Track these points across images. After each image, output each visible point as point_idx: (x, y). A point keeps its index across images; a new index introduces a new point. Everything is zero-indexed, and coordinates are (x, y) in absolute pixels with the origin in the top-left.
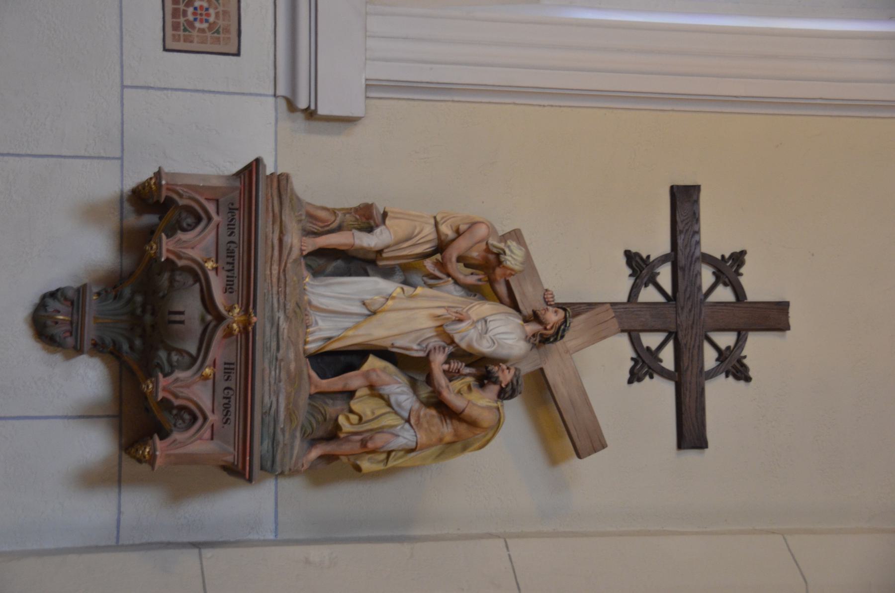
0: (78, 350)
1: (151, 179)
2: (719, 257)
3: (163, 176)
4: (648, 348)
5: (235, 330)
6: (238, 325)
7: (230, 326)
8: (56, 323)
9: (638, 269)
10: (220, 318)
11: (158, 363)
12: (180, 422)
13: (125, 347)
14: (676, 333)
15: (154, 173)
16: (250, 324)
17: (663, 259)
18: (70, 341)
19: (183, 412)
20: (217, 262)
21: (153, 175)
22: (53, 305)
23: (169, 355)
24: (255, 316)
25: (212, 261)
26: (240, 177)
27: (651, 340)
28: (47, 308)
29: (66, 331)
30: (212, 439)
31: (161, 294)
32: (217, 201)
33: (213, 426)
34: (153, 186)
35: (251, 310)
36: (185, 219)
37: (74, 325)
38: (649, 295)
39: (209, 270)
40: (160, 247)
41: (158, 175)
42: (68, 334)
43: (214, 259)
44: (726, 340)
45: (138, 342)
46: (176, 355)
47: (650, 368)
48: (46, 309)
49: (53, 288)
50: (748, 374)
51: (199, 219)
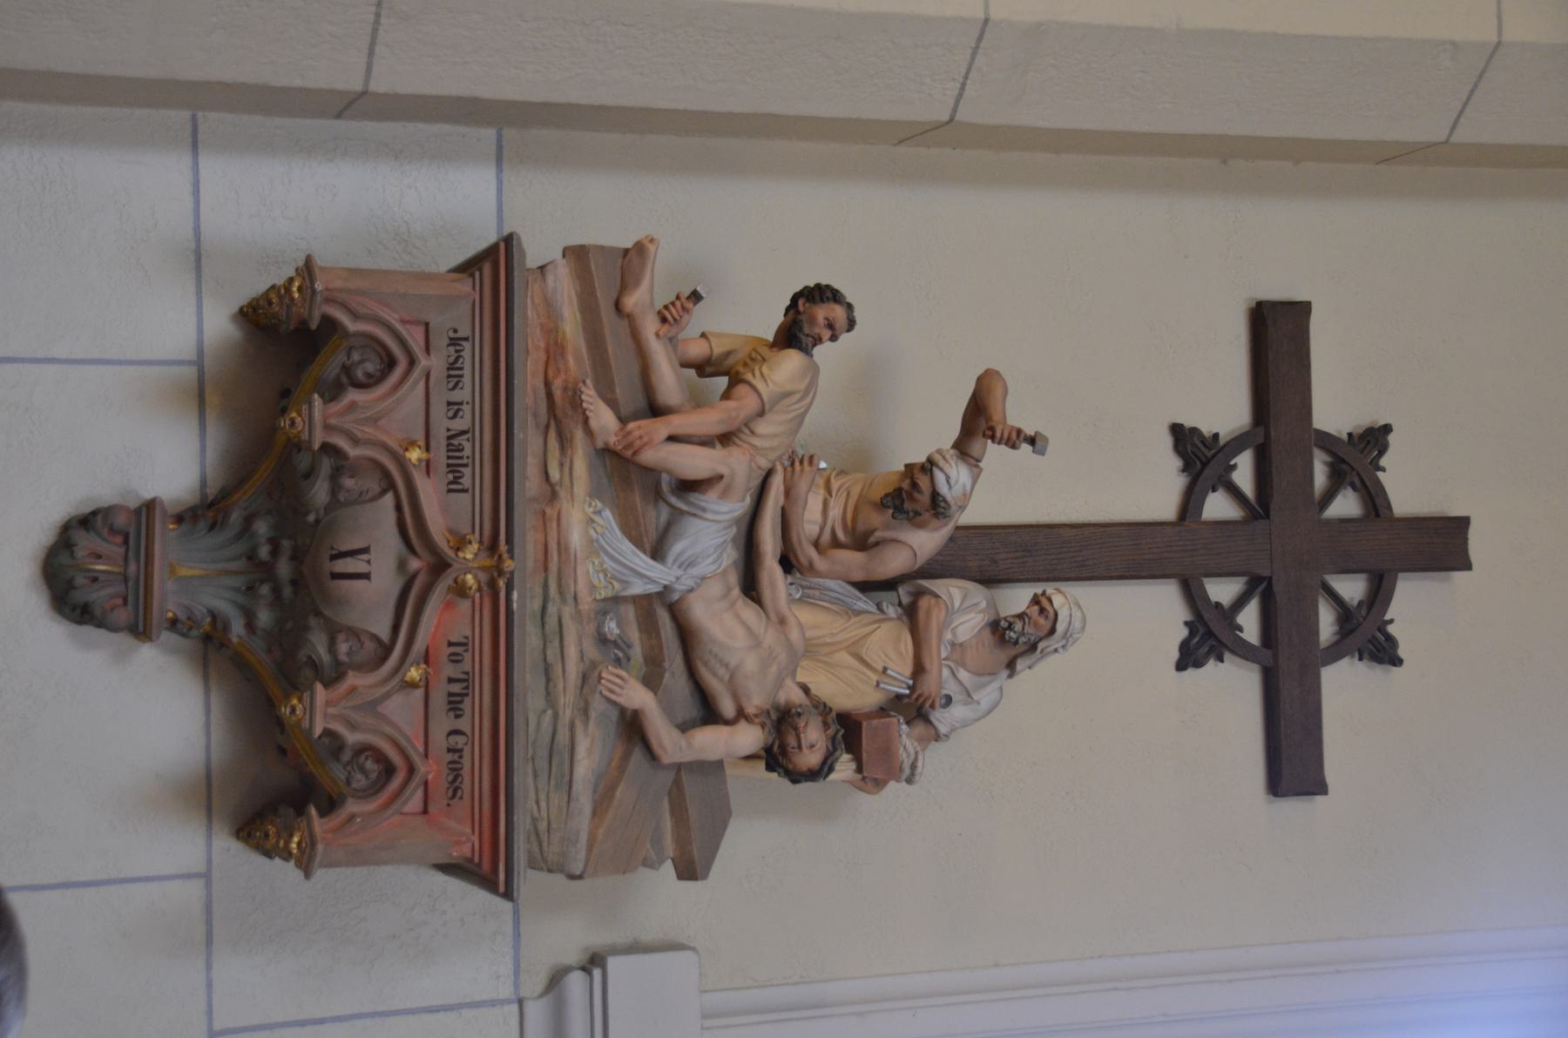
0: (141, 630)
1: (291, 280)
3: (317, 272)
4: (1218, 605)
5: (470, 588)
6: (475, 577)
7: (459, 580)
8: (95, 580)
9: (1198, 463)
12: (359, 776)
13: (237, 629)
14: (1270, 578)
15: (297, 270)
16: (501, 573)
17: (1238, 443)
19: (362, 758)
20: (428, 449)
22: (85, 542)
24: (512, 558)
25: (420, 447)
26: (472, 275)
27: (1222, 591)
29: (116, 596)
30: (425, 811)
31: (311, 518)
32: (427, 325)
35: (503, 547)
36: (362, 361)
37: (130, 584)
38: (1218, 507)
39: (414, 465)
42: (119, 601)
43: (422, 443)
44: (1352, 588)
45: (264, 617)
46: (347, 640)
48: (72, 552)
49: (87, 510)
51: (391, 363)
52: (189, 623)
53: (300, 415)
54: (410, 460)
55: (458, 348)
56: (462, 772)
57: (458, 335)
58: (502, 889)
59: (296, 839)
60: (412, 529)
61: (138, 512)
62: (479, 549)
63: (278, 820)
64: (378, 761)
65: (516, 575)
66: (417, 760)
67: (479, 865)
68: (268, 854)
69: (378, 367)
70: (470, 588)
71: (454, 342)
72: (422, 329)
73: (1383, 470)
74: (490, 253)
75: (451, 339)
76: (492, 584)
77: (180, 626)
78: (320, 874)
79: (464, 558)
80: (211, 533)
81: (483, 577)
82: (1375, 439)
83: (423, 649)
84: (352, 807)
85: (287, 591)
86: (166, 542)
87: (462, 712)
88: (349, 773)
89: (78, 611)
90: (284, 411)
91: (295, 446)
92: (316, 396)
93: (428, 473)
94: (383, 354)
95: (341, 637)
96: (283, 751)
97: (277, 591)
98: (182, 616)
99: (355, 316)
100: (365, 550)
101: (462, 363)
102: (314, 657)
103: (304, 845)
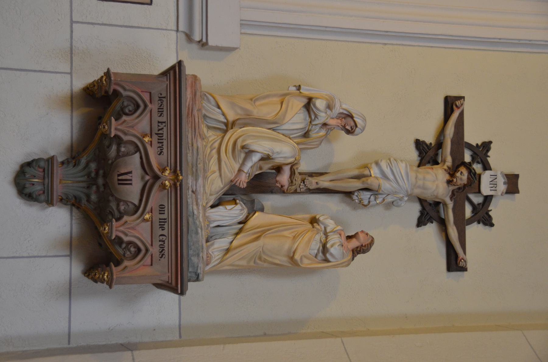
0: (50, 203)
1: (102, 77)
2: (475, 145)
5: (167, 186)
6: (169, 182)
7: (163, 183)
8: (33, 184)
10: (156, 178)
11: (110, 212)
12: (128, 253)
13: (84, 201)
15: (104, 73)
16: (178, 180)
18: (42, 197)
20: (151, 137)
21: (103, 75)
23: (118, 205)
24: (182, 175)
25: (148, 136)
26: (166, 75)
28: (26, 174)
30: (152, 265)
31: (110, 162)
32: (150, 93)
33: (152, 255)
34: (104, 82)
35: (179, 172)
36: (128, 106)
37: (46, 186)
39: (147, 143)
40: (110, 128)
41: (108, 74)
43: (149, 135)
45: (93, 197)
47: (431, 217)
49: (30, 159)
50: (492, 221)
51: (138, 106)
52: (67, 200)
53: (107, 124)
54: (145, 141)
55: (162, 101)
56: (163, 113)
57: (162, 96)
58: (179, 292)
59: (106, 275)
60: (146, 165)
61: (48, 160)
62: (170, 172)
63: (99, 269)
64: (135, 248)
65: (183, 181)
66: (148, 102)
67: (171, 283)
68: (96, 281)
69: (133, 108)
70: (167, 186)
71: (161, 99)
72: (148, 94)
73: (489, 157)
74: (173, 68)
75: (160, 98)
76: (175, 185)
77: (63, 201)
78: (115, 287)
79: (165, 175)
80: (74, 168)
81: (172, 182)
82: (486, 146)
83: (151, 207)
84: (126, 263)
85: (102, 189)
86: (59, 172)
87: (164, 228)
88: (125, 252)
89: (27, 196)
90: (100, 124)
91: (105, 136)
92: (112, 117)
93: (151, 145)
94: (134, 102)
95: (122, 203)
96: (100, 245)
97: (98, 187)
98: (64, 197)
99: (125, 89)
100: (130, 172)
101: (163, 106)
102: (111, 210)
103: (109, 277)
